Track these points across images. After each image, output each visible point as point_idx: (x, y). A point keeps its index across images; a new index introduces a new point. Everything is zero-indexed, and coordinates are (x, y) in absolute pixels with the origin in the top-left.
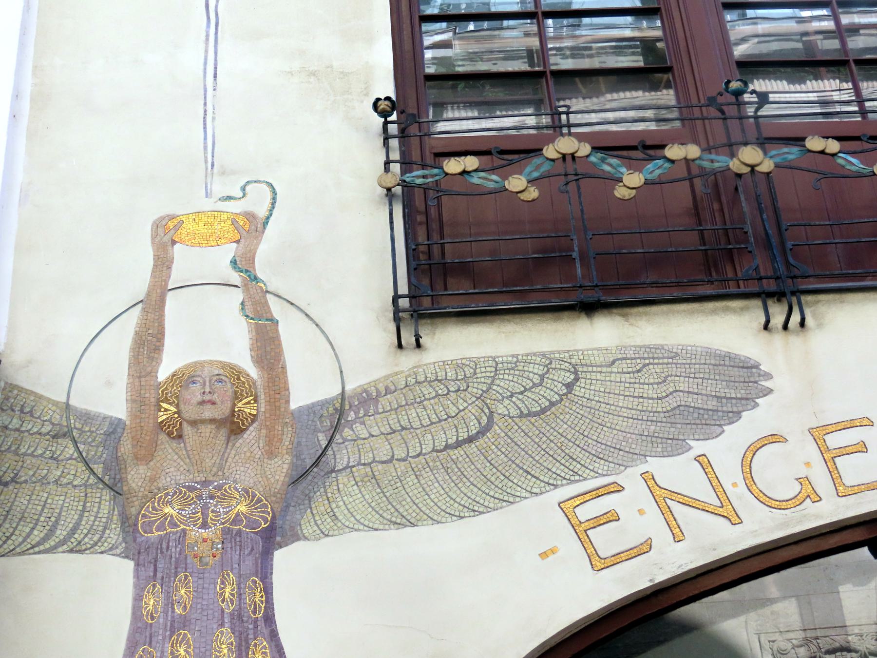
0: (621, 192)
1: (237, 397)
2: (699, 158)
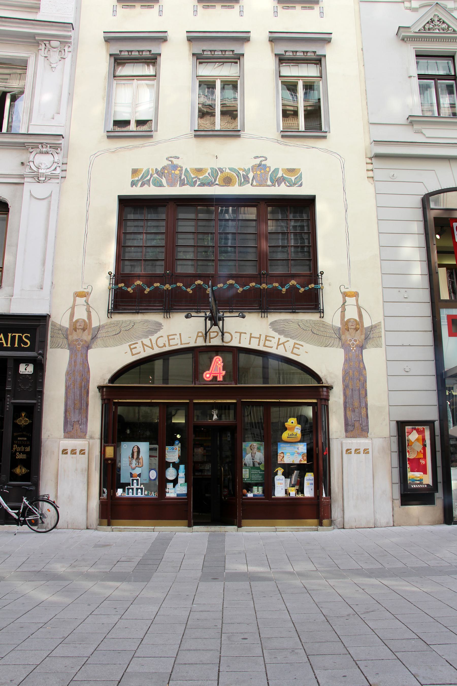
0: (146, 292)
1: (84, 325)
2: (159, 286)
